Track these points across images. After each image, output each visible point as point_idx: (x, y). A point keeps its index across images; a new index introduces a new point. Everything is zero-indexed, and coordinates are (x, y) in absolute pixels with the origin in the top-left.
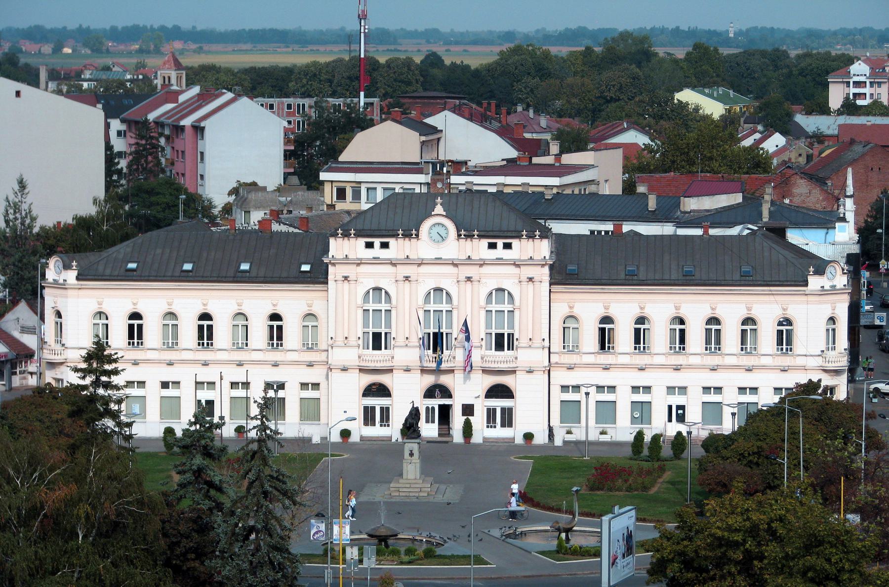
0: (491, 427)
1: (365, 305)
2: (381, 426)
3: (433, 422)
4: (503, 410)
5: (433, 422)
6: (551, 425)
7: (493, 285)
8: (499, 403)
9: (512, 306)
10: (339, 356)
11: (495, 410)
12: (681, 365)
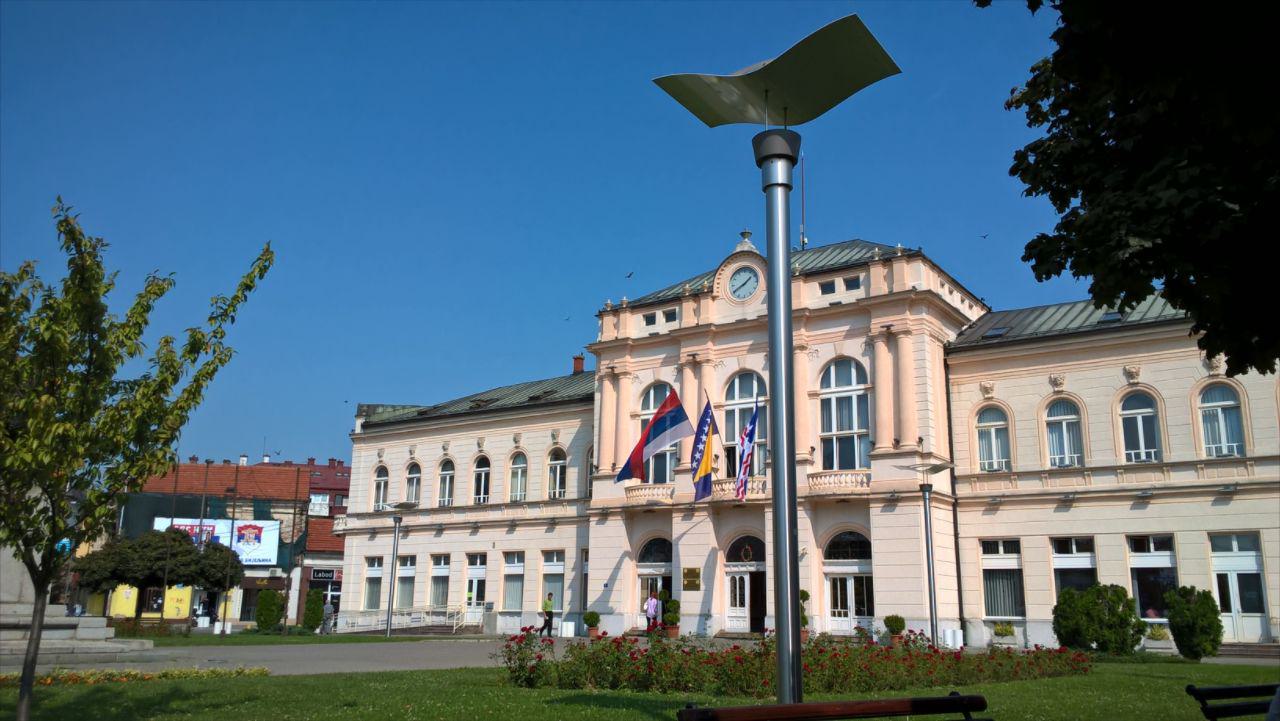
0: (840, 615)
3: (742, 604)
5: (742, 604)
6: (966, 615)
7: (828, 353)
8: (849, 568)
11: (844, 582)
12: (1237, 484)
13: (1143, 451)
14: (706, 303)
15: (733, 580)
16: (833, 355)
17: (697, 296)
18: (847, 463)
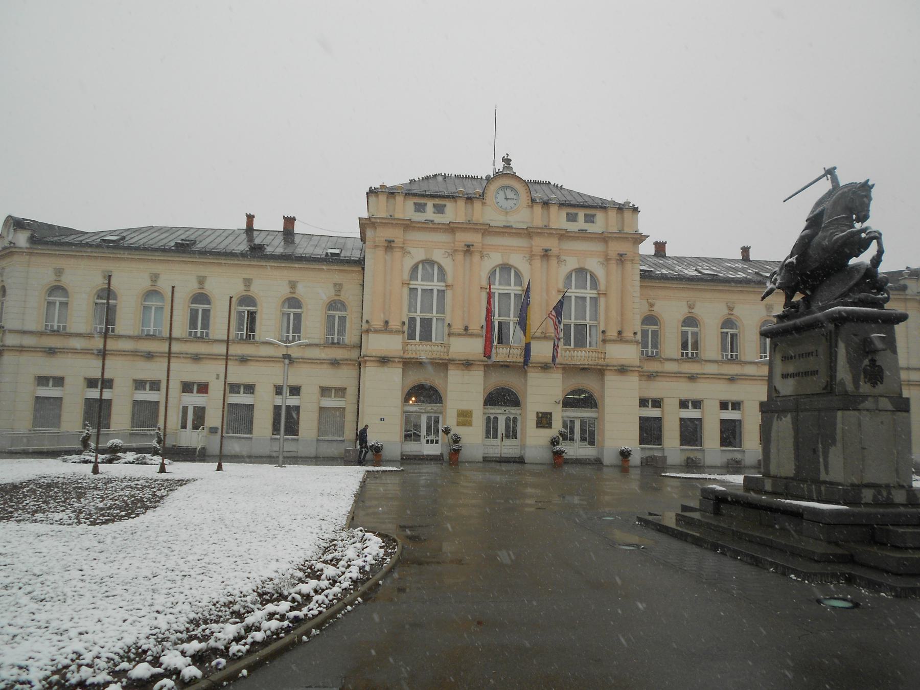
1: (412, 282)
2: (428, 441)
4: (583, 423)
9: (595, 292)
10: (377, 344)
11: (572, 422)
13: (690, 351)
14: (477, 205)
15: (488, 419)
16: (577, 266)
17: (469, 199)
18: (580, 343)
